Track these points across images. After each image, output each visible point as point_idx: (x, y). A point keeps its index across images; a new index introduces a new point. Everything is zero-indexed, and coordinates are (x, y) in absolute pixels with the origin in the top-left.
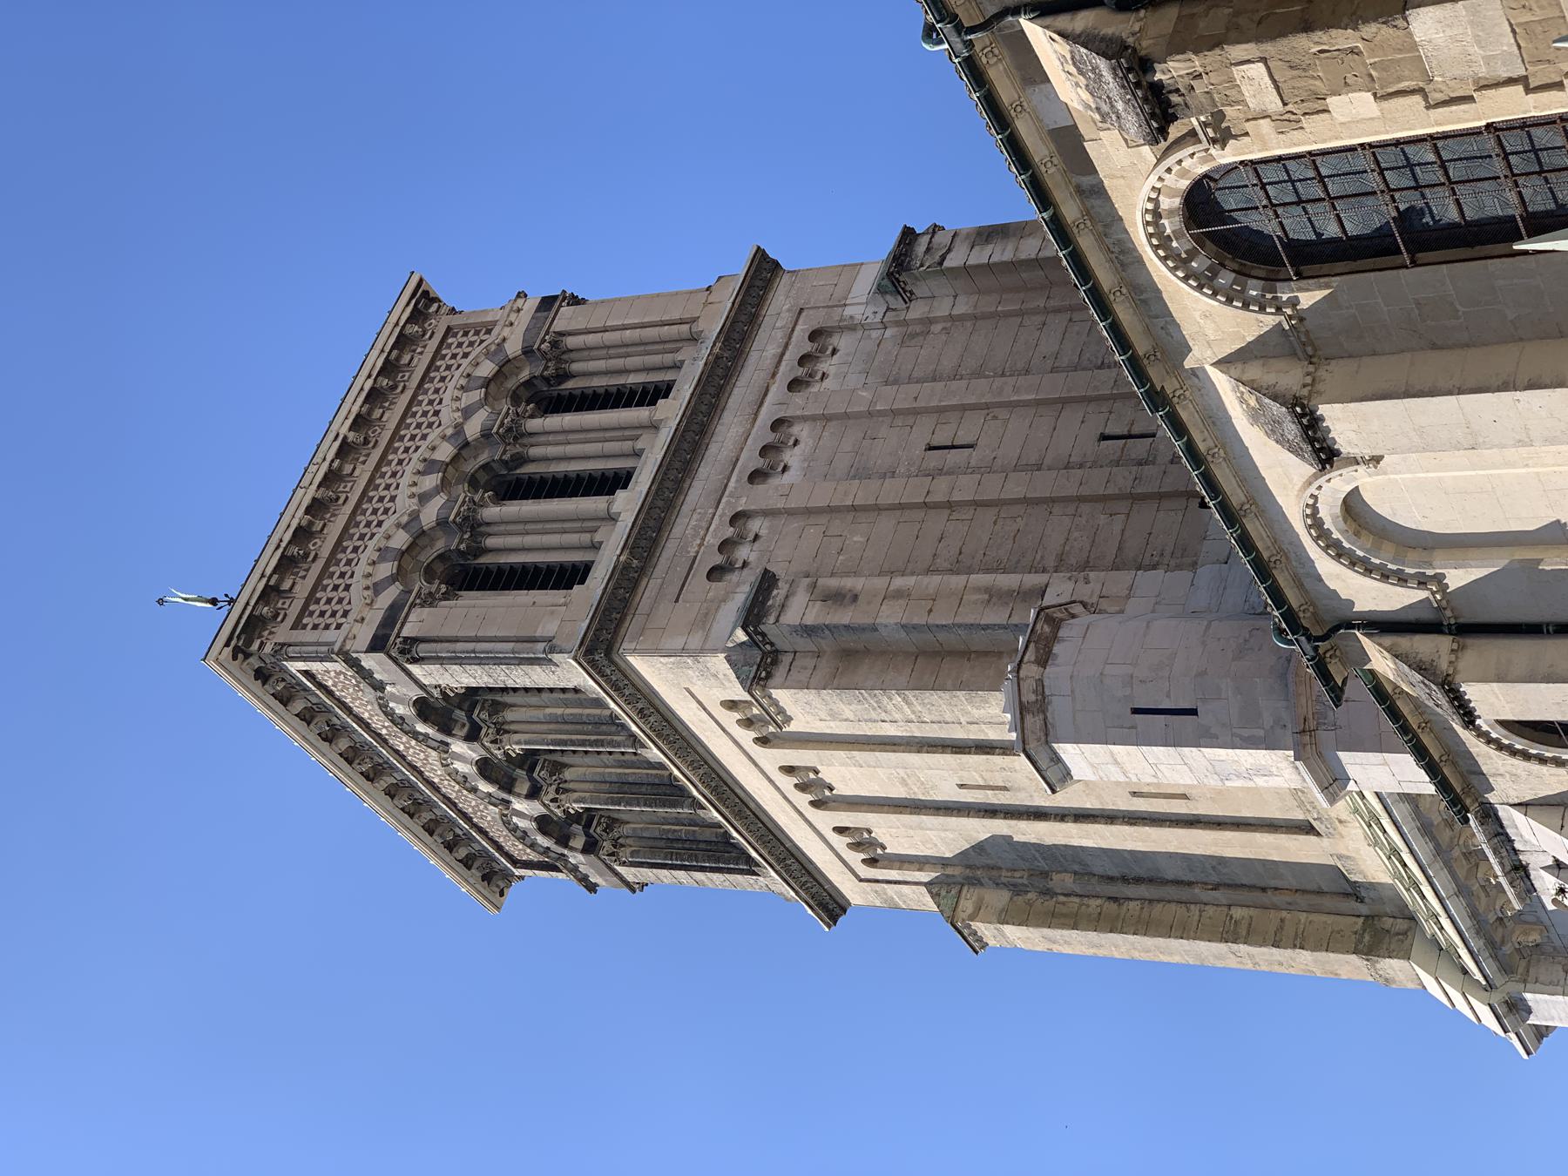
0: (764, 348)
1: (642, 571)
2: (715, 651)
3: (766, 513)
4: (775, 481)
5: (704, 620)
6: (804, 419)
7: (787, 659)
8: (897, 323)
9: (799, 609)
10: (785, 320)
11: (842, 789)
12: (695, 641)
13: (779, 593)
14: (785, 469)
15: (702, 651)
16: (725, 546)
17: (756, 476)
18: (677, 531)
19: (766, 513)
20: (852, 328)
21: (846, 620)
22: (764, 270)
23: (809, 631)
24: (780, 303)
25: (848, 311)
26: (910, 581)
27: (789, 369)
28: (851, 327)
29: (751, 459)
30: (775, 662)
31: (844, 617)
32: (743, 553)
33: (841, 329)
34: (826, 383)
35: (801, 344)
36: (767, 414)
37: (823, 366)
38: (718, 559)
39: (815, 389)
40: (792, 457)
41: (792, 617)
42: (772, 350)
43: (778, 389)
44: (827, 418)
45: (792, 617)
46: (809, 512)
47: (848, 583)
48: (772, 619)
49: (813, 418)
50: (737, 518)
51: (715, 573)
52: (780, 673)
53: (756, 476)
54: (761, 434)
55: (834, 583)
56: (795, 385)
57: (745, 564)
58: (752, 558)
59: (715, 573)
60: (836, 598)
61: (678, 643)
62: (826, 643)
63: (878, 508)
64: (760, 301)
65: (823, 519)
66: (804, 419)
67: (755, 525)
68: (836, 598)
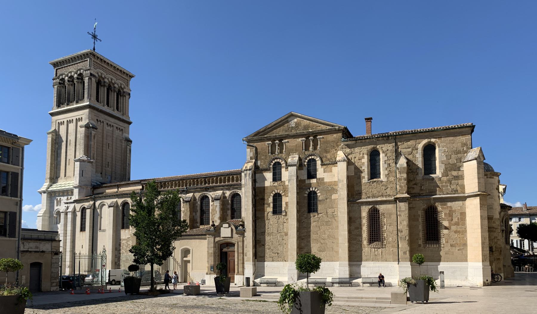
0: (121, 124)
1: (98, 111)
2: (89, 121)
3: (103, 125)
4: (107, 125)
5: (92, 119)
6: (113, 129)
7: (88, 129)
8: (122, 139)
9: (93, 133)
10: (124, 126)
11: (69, 125)
12: (90, 118)
13: (95, 130)
14: (108, 127)
15: (89, 119)
16: (100, 121)
17: (107, 124)
18: (102, 115)
19: (103, 125)
20: (122, 134)
21: (92, 138)
22: (130, 123)
23: (91, 133)
24: (126, 125)
25: (124, 133)
26: (96, 145)
27: (119, 127)
28: (122, 134)
29: (109, 123)
30: (87, 128)
31: (92, 138)
32: (99, 123)
33: (122, 132)
34: (117, 131)
35: (121, 128)
36: (114, 125)
37: (118, 130)
38: (99, 120)
39: (116, 130)
40: (109, 127)
41: (93, 132)
42: (121, 125)
43: (116, 126)
44: (113, 132)
45: (93, 132)
46: (103, 130)
47: (96, 138)
48: (93, 130)
49: (113, 130)
50: (103, 122)
51: (97, 120)
52: (86, 129)
53: (107, 124)
54: (112, 124)
55: (96, 136)
56: (117, 128)
57: (98, 123)
58: (99, 124)
59: (97, 120)
60: (94, 137)
61: (90, 116)
62: (89, 134)
63: (103, 138)
64: (126, 123)
65: (102, 132)
66: (113, 129)
67: (102, 124)
68: (94, 137)
